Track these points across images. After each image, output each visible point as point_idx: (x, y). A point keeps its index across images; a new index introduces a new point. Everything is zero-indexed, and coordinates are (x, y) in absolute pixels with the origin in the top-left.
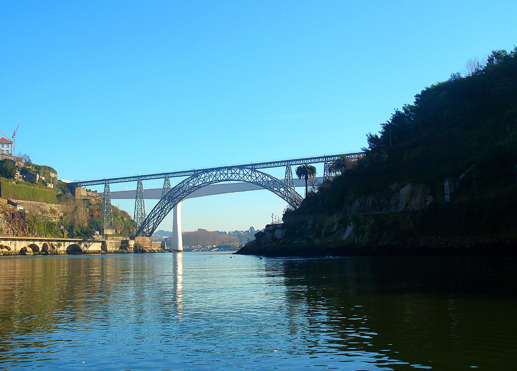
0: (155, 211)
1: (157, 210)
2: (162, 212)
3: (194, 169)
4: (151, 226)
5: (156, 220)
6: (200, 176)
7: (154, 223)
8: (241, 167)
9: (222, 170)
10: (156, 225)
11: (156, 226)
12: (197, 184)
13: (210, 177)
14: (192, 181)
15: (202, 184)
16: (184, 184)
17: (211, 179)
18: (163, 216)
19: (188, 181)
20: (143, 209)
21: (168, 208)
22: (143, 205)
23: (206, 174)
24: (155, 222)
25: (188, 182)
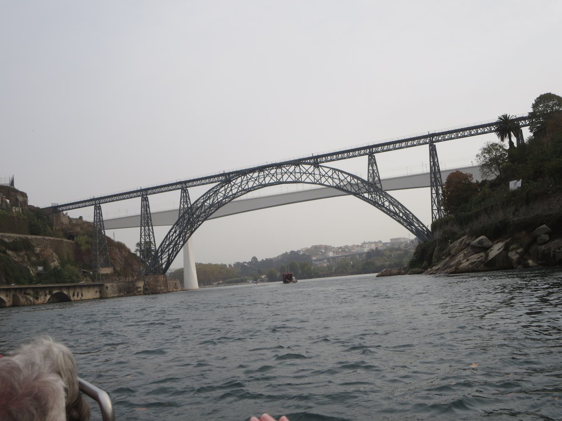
1: (173, 235)
2: (180, 237)
3: (224, 171)
4: (165, 259)
5: (171, 250)
6: (234, 181)
7: (169, 254)
8: (297, 163)
9: (266, 170)
10: (172, 257)
11: (172, 258)
12: (230, 194)
13: (250, 180)
14: (223, 188)
15: (237, 192)
16: (211, 194)
17: (251, 184)
18: (182, 243)
19: (215, 190)
20: (151, 236)
21: (188, 232)
22: (151, 230)
24: (170, 252)
25: (216, 191)
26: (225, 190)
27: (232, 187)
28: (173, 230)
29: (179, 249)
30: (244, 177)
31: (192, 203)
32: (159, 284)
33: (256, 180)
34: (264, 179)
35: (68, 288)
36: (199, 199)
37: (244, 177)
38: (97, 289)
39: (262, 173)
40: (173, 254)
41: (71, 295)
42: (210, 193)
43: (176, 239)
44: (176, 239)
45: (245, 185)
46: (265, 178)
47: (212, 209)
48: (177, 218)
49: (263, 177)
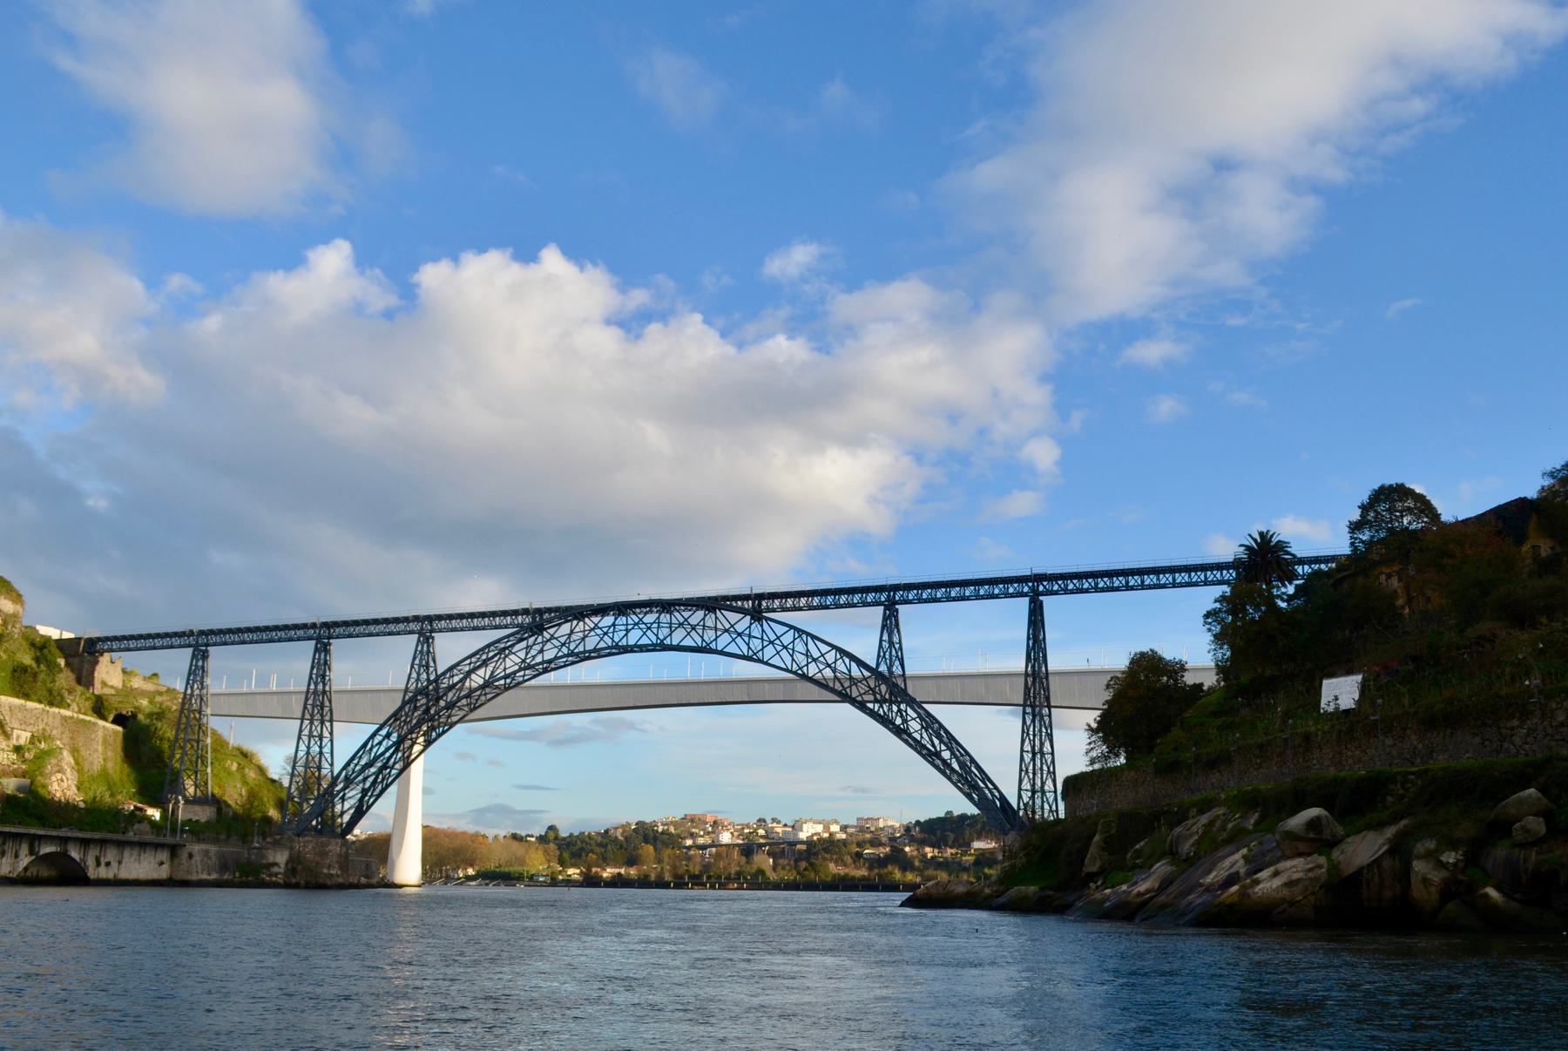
0: (372, 747)
1: (380, 743)
2: (396, 751)
3: (531, 604)
4: (352, 802)
5: (371, 779)
6: (551, 631)
7: (363, 790)
8: (711, 604)
9: (634, 613)
10: (370, 797)
11: (369, 799)
12: (539, 659)
13: (592, 633)
14: (524, 644)
15: (556, 658)
16: (491, 654)
17: (591, 643)
19: (503, 646)
20: (325, 741)
23: (575, 622)
24: (368, 784)
25: (505, 649)
26: (527, 648)
27: (544, 643)
28: (384, 732)
29: (389, 781)
30: (577, 624)
31: (439, 673)
32: (328, 861)
33: (605, 634)
34: (626, 635)
35: (85, 843)
36: (458, 664)
37: (577, 624)
38: (164, 855)
39: (624, 618)
40: (374, 790)
41: (91, 862)
42: (489, 651)
43: (388, 754)
44: (388, 754)
45: (577, 642)
46: (627, 631)
47: (488, 690)
48: (398, 704)
49: (623, 627)
